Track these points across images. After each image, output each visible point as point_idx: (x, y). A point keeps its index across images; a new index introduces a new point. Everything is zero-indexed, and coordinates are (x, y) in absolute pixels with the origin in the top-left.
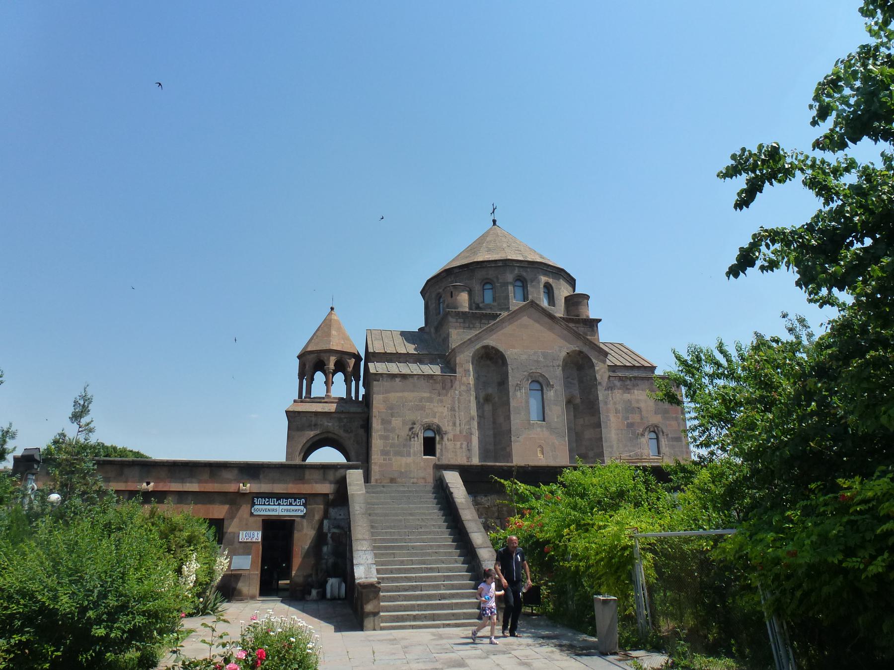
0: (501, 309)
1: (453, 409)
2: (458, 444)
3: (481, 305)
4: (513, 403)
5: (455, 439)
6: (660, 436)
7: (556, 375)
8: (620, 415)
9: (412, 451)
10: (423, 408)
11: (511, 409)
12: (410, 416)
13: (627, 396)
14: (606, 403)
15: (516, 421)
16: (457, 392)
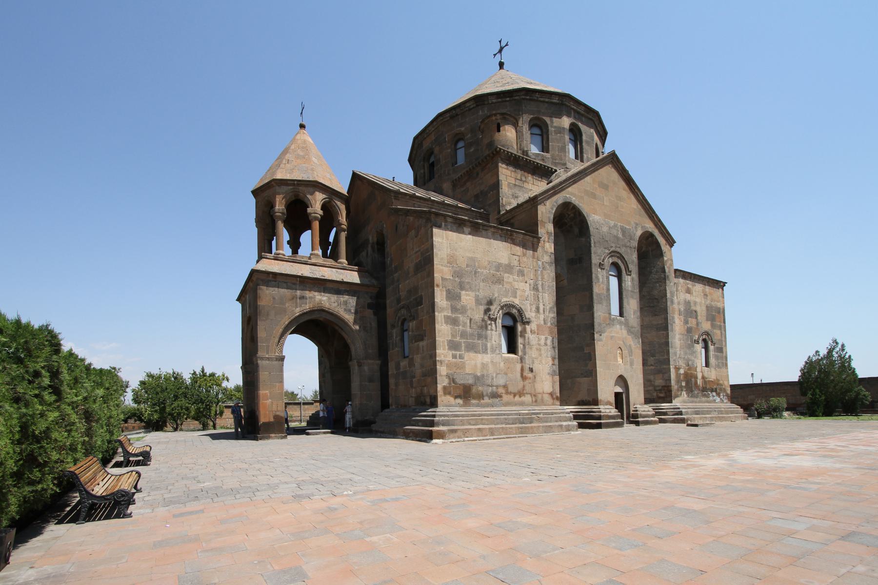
0: (556, 164)
1: (535, 288)
2: (543, 337)
3: (530, 154)
4: (596, 290)
5: (538, 331)
6: (710, 343)
7: (632, 258)
8: (682, 318)
9: (489, 345)
10: (500, 281)
11: (595, 297)
12: (485, 292)
13: (688, 297)
14: (672, 302)
15: (599, 313)
16: (540, 263)
